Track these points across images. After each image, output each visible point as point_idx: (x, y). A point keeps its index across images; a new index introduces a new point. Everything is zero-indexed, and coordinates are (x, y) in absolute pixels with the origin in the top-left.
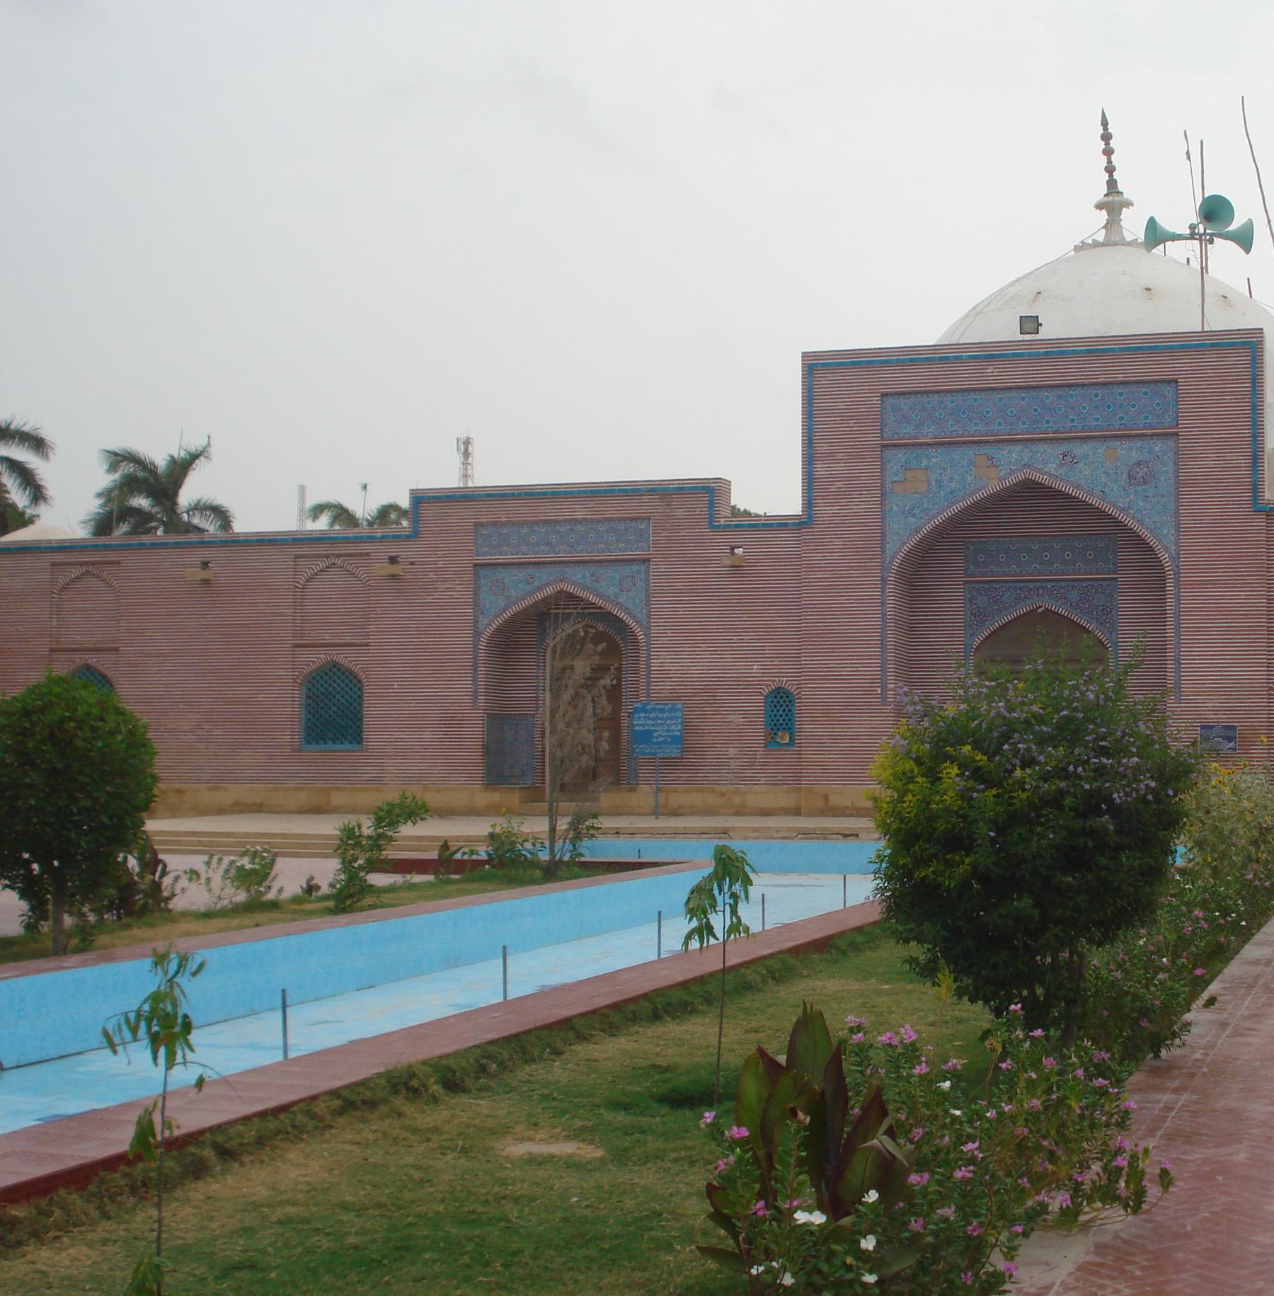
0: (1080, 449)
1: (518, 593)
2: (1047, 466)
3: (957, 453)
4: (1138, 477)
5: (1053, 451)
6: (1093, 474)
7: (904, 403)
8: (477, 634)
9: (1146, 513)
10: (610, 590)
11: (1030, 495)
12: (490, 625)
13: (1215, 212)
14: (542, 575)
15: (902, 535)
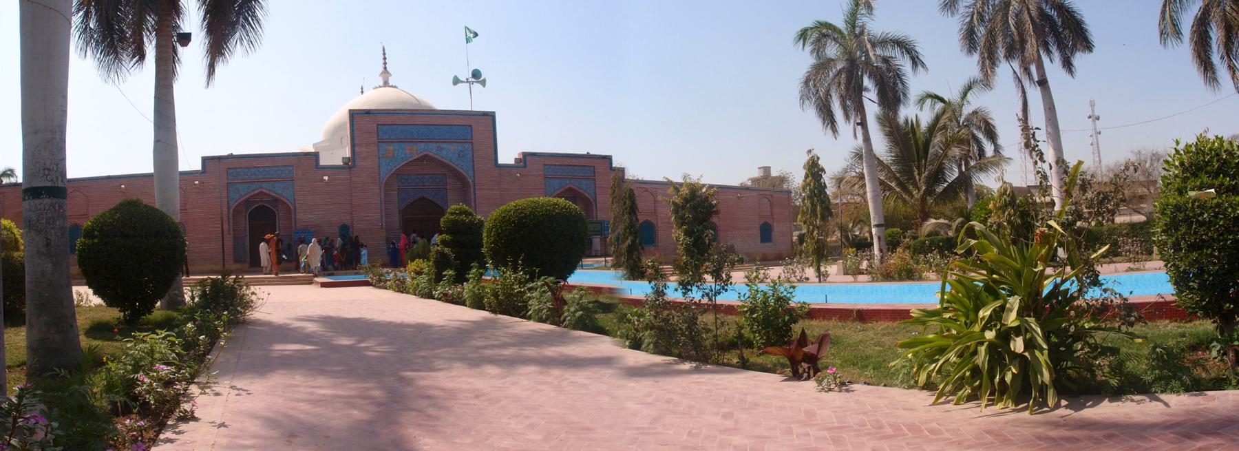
0: (443, 146)
1: (244, 192)
2: (432, 149)
3: (403, 145)
4: (461, 155)
5: (434, 146)
6: (448, 153)
7: (385, 128)
8: (229, 208)
9: (463, 167)
10: (279, 190)
11: (425, 158)
12: (233, 205)
13: (476, 74)
14: (254, 186)
15: (385, 172)
